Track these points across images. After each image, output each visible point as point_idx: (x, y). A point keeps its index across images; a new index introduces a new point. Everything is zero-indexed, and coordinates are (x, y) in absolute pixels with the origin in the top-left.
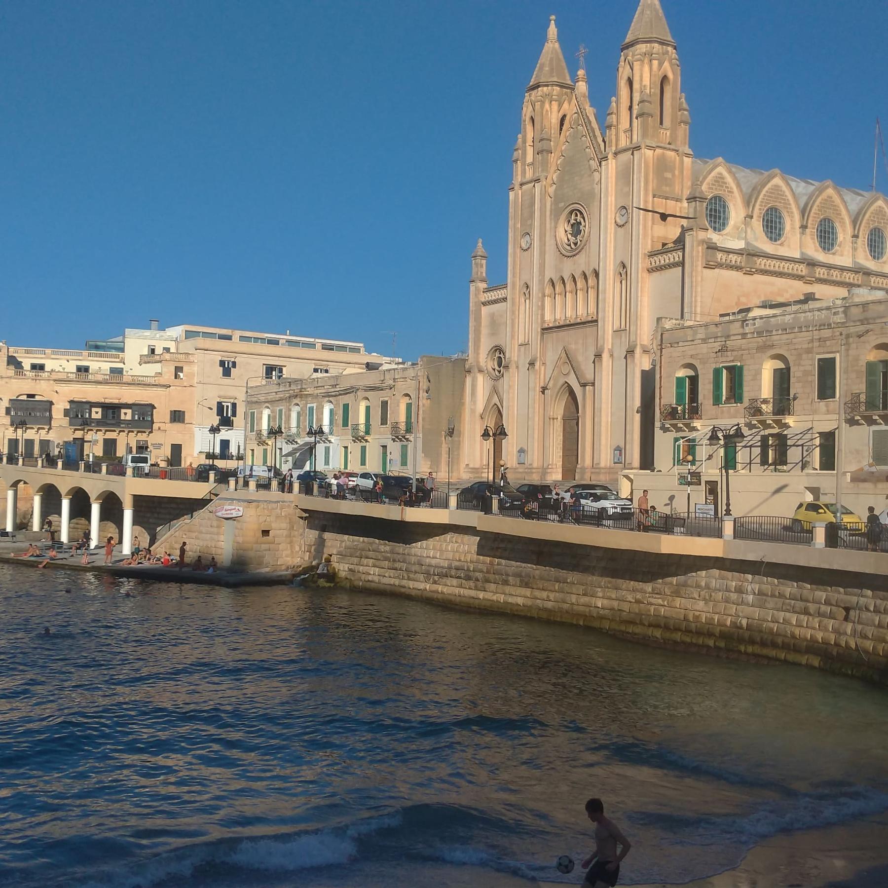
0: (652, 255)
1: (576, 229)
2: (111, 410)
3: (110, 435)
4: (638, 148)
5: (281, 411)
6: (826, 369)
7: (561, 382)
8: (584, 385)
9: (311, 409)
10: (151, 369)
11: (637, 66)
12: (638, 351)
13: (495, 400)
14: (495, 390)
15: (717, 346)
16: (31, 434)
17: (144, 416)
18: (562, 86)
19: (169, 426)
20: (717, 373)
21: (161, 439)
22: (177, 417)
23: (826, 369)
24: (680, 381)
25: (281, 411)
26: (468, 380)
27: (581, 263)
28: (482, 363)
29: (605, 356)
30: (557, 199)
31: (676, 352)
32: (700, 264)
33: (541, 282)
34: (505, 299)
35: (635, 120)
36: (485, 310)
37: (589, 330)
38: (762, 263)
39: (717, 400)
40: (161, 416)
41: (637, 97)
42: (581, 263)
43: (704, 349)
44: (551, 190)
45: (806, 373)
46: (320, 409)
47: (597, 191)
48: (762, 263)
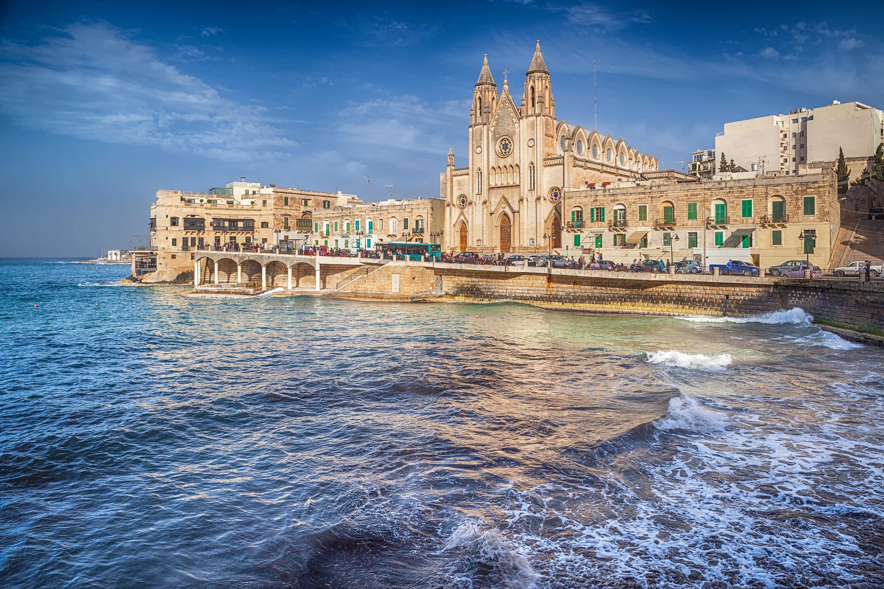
0: (545, 160)
1: (505, 147)
2: (233, 222)
3: (218, 235)
4: (539, 115)
5: (336, 223)
6: (643, 210)
7: (501, 210)
8: (514, 213)
9: (357, 222)
10: (247, 202)
11: (536, 82)
12: (542, 199)
13: (462, 218)
14: (462, 213)
15: (592, 200)
16: (195, 235)
17: (249, 225)
18: (492, 85)
19: (261, 229)
20: (592, 210)
21: (259, 234)
22: (265, 225)
23: (643, 210)
24: (573, 212)
25: (336, 223)
26: (448, 209)
27: (509, 161)
28: (455, 202)
29: (525, 200)
30: (494, 133)
31: (572, 201)
32: (571, 165)
33: (488, 168)
34: (468, 174)
35: (536, 105)
36: (455, 179)
37: (514, 189)
38: (589, 165)
39: (592, 221)
40: (257, 224)
41: (537, 95)
42: (509, 161)
43: (586, 200)
44: (492, 129)
45: (634, 211)
46: (364, 220)
47: (517, 131)
48: (589, 165)
